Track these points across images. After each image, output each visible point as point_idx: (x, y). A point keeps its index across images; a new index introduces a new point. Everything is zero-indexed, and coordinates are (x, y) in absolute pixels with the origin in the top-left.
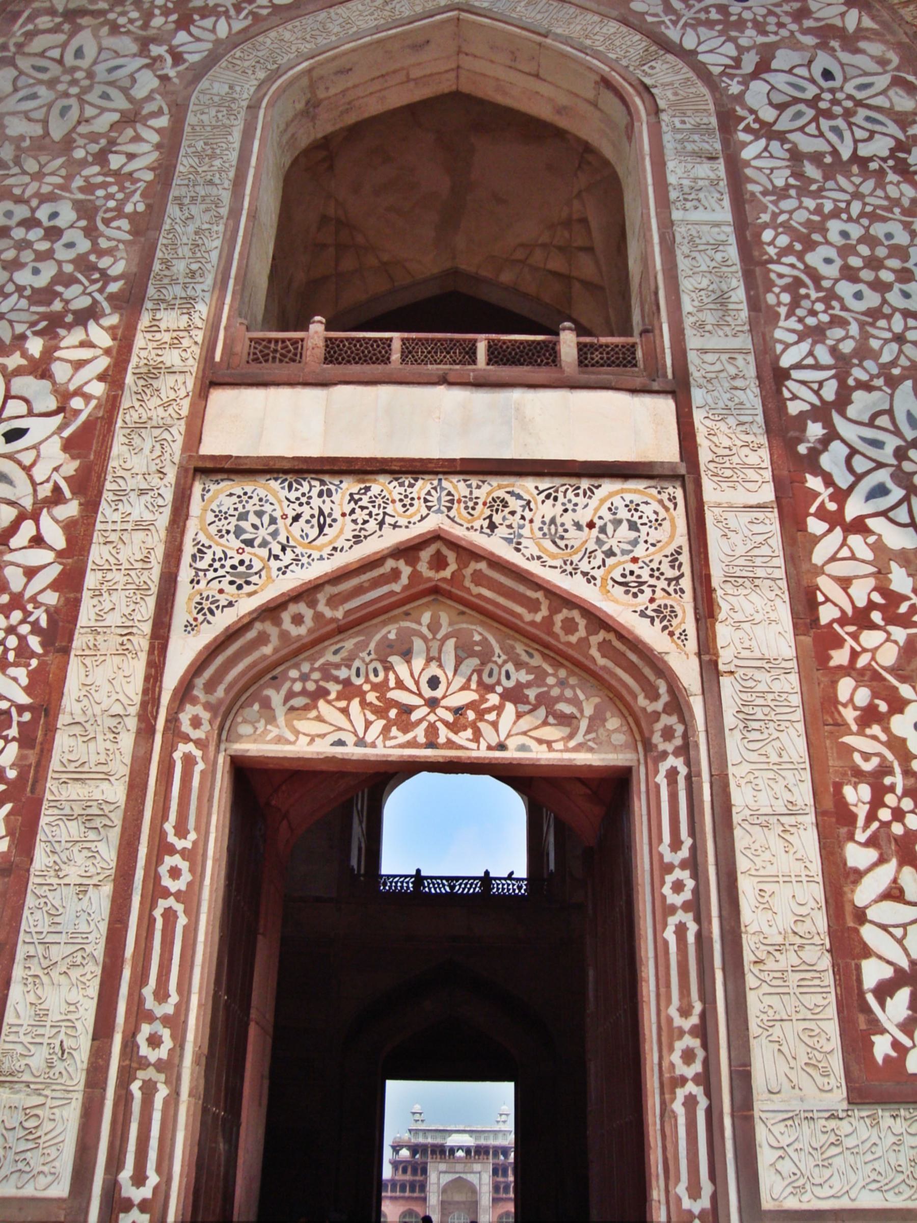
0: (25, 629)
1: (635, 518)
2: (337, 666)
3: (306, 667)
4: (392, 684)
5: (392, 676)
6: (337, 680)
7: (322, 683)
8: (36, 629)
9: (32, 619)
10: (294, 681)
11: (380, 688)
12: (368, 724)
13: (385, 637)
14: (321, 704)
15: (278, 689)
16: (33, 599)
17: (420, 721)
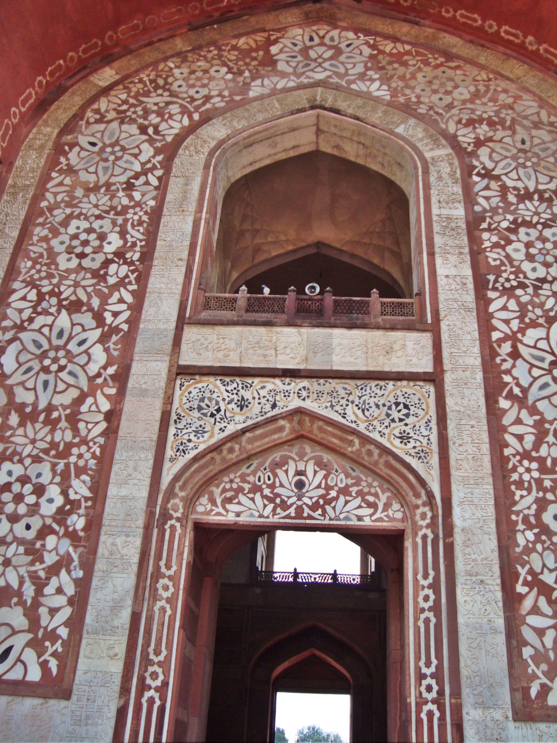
0: (87, 456)
1: (407, 403)
2: (248, 475)
3: (232, 476)
4: (277, 484)
5: (277, 480)
6: (249, 483)
7: (240, 484)
8: (94, 456)
9: (92, 451)
10: (226, 483)
11: (272, 487)
12: (265, 506)
13: (274, 459)
14: (240, 495)
15: (218, 487)
16: (92, 440)
17: (292, 505)
